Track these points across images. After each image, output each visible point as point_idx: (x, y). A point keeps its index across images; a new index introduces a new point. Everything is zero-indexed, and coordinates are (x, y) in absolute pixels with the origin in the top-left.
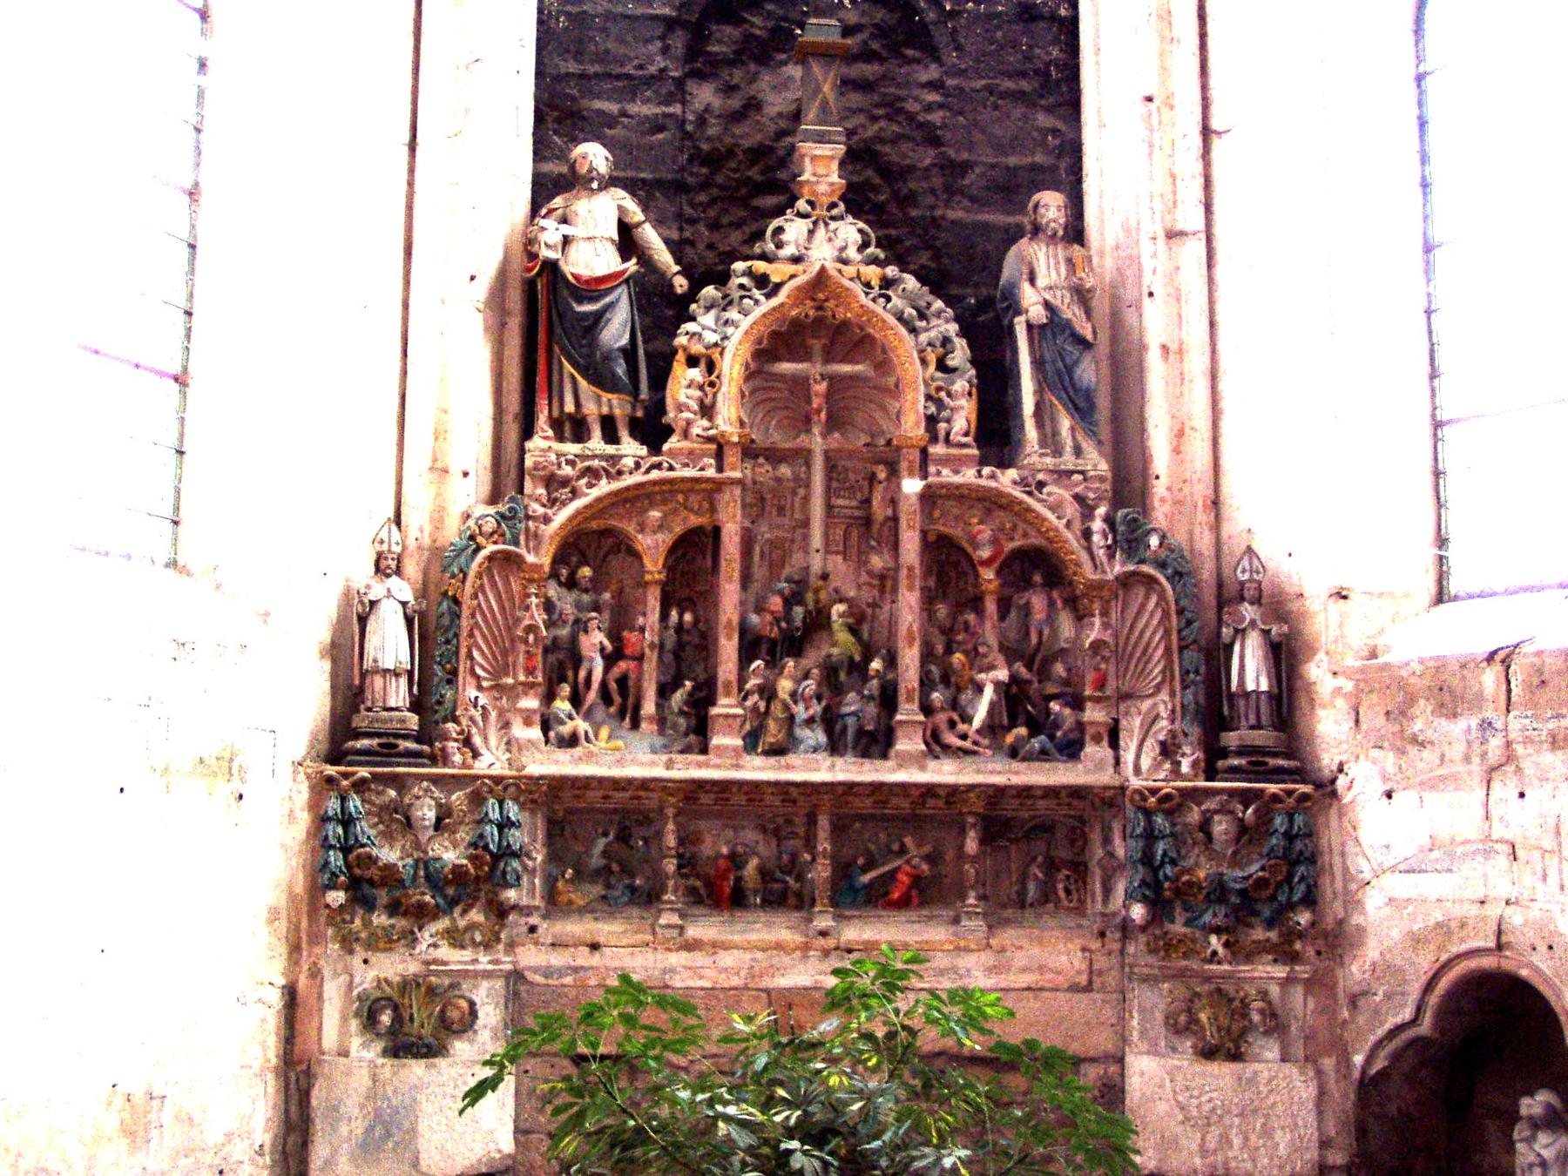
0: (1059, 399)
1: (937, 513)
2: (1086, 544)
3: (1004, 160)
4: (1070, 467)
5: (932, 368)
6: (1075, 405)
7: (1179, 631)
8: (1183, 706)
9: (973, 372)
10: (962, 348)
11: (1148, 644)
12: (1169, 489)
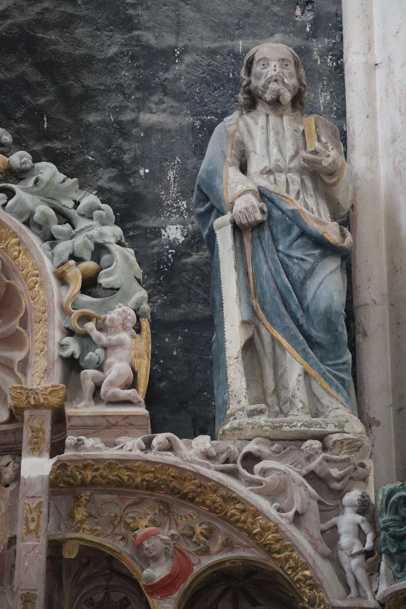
0: (285, 330)
1: (80, 514)
2: (328, 551)
3: (229, 43)
4: (299, 428)
5: (76, 285)
6: (308, 338)
9: (142, 293)
10: (126, 258)
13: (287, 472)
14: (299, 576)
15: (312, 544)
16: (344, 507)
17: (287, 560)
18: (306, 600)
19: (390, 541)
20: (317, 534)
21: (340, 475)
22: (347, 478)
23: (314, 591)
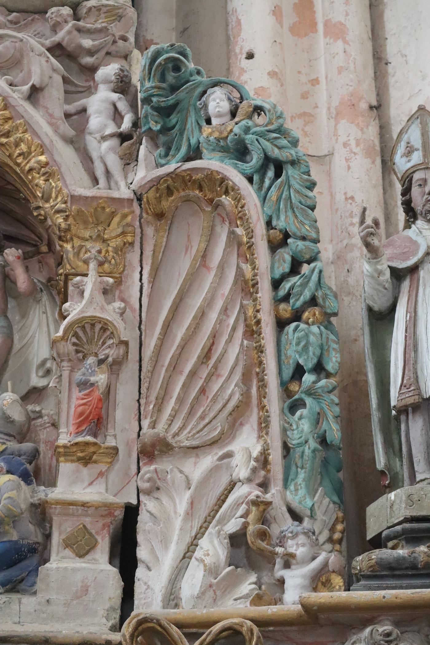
2: (71, 133)
7: (276, 284)
8: (286, 449)
11: (214, 336)
12: (272, 74)
13: (24, 40)
14: (32, 163)
15: (51, 124)
16: (96, 88)
17: (17, 145)
18: (40, 195)
19: (153, 115)
20: (59, 113)
21: (93, 45)
22: (103, 53)
23: (51, 181)
